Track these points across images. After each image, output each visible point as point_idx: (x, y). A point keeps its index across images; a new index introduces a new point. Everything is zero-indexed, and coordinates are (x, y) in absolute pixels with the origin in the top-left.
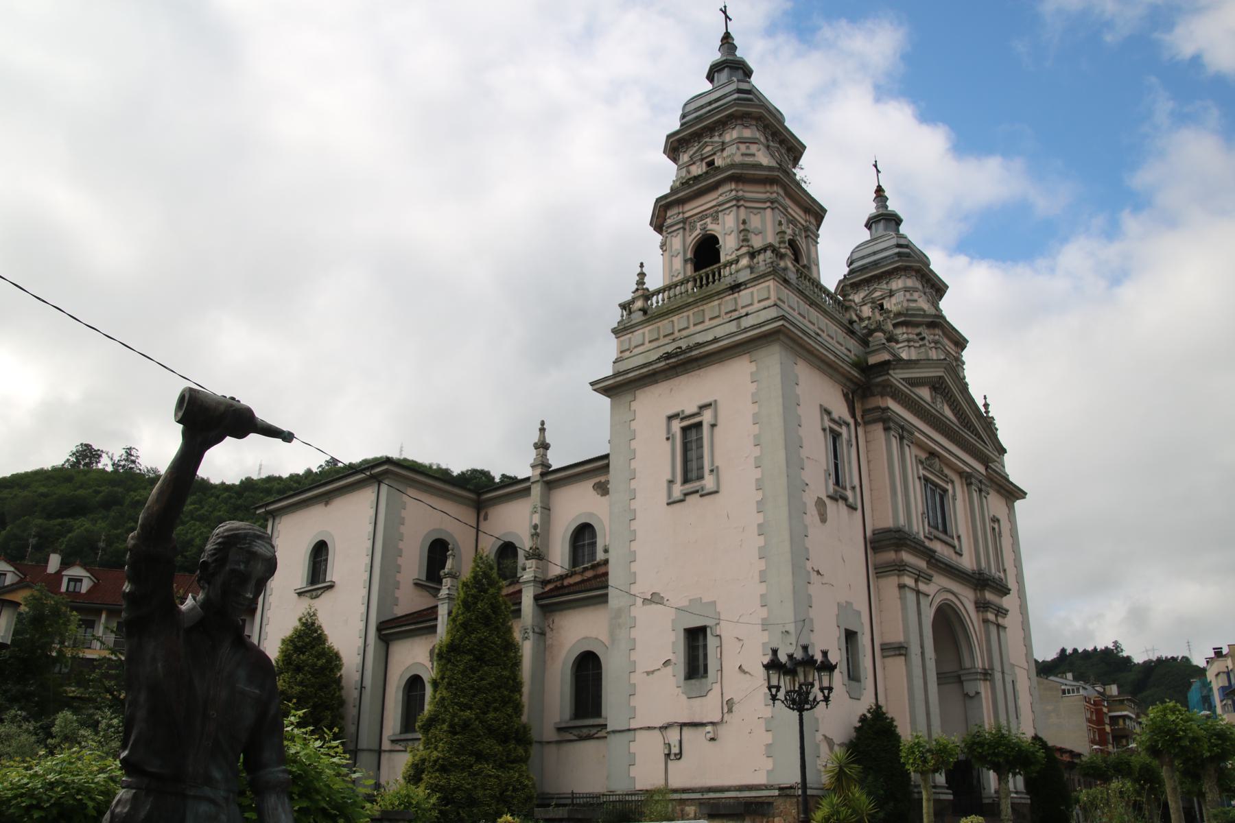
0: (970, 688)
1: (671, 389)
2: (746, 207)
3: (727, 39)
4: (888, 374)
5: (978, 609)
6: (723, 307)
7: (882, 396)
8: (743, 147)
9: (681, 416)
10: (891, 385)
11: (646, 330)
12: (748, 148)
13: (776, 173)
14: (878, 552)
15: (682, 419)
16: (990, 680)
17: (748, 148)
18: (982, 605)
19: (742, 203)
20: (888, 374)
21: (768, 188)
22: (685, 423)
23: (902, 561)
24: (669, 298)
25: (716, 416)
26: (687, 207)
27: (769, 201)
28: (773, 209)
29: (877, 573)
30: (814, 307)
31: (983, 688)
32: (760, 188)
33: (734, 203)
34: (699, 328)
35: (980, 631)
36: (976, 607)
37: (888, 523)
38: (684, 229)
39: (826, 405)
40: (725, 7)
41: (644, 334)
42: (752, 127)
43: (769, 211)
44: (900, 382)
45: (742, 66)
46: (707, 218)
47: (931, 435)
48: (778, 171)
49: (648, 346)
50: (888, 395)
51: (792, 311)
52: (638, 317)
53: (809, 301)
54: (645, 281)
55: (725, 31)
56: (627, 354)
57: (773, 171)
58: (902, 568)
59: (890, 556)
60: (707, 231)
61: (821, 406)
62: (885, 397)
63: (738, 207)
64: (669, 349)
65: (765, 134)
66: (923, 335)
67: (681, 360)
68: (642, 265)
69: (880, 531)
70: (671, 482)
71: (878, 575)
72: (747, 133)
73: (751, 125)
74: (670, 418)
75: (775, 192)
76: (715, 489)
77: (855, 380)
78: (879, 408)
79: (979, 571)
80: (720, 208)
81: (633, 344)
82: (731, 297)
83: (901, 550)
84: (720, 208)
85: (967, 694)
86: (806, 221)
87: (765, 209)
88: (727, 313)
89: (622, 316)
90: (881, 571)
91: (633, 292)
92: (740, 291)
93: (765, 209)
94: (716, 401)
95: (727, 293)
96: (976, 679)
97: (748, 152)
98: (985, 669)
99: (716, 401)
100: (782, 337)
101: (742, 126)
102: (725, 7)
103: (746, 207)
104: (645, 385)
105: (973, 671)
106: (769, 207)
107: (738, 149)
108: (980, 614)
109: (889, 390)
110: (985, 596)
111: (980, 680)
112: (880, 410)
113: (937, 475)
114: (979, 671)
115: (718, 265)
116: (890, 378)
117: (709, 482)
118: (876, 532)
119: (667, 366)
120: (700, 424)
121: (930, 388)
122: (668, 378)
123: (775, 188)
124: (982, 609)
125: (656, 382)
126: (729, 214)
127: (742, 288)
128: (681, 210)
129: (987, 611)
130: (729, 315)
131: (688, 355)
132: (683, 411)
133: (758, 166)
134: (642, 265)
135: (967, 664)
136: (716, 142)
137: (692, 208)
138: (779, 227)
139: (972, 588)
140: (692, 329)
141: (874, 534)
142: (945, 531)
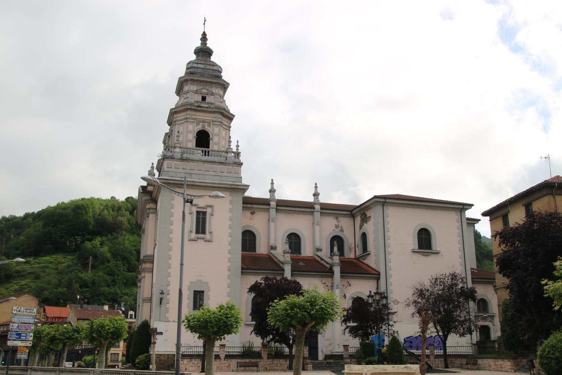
2: (178, 124)
19: (177, 123)
28: (186, 122)
43: (185, 123)
63: (175, 125)
87: (184, 122)
93: (184, 122)
103: (178, 124)
107: (183, 97)
123: (188, 112)
126: (181, 126)
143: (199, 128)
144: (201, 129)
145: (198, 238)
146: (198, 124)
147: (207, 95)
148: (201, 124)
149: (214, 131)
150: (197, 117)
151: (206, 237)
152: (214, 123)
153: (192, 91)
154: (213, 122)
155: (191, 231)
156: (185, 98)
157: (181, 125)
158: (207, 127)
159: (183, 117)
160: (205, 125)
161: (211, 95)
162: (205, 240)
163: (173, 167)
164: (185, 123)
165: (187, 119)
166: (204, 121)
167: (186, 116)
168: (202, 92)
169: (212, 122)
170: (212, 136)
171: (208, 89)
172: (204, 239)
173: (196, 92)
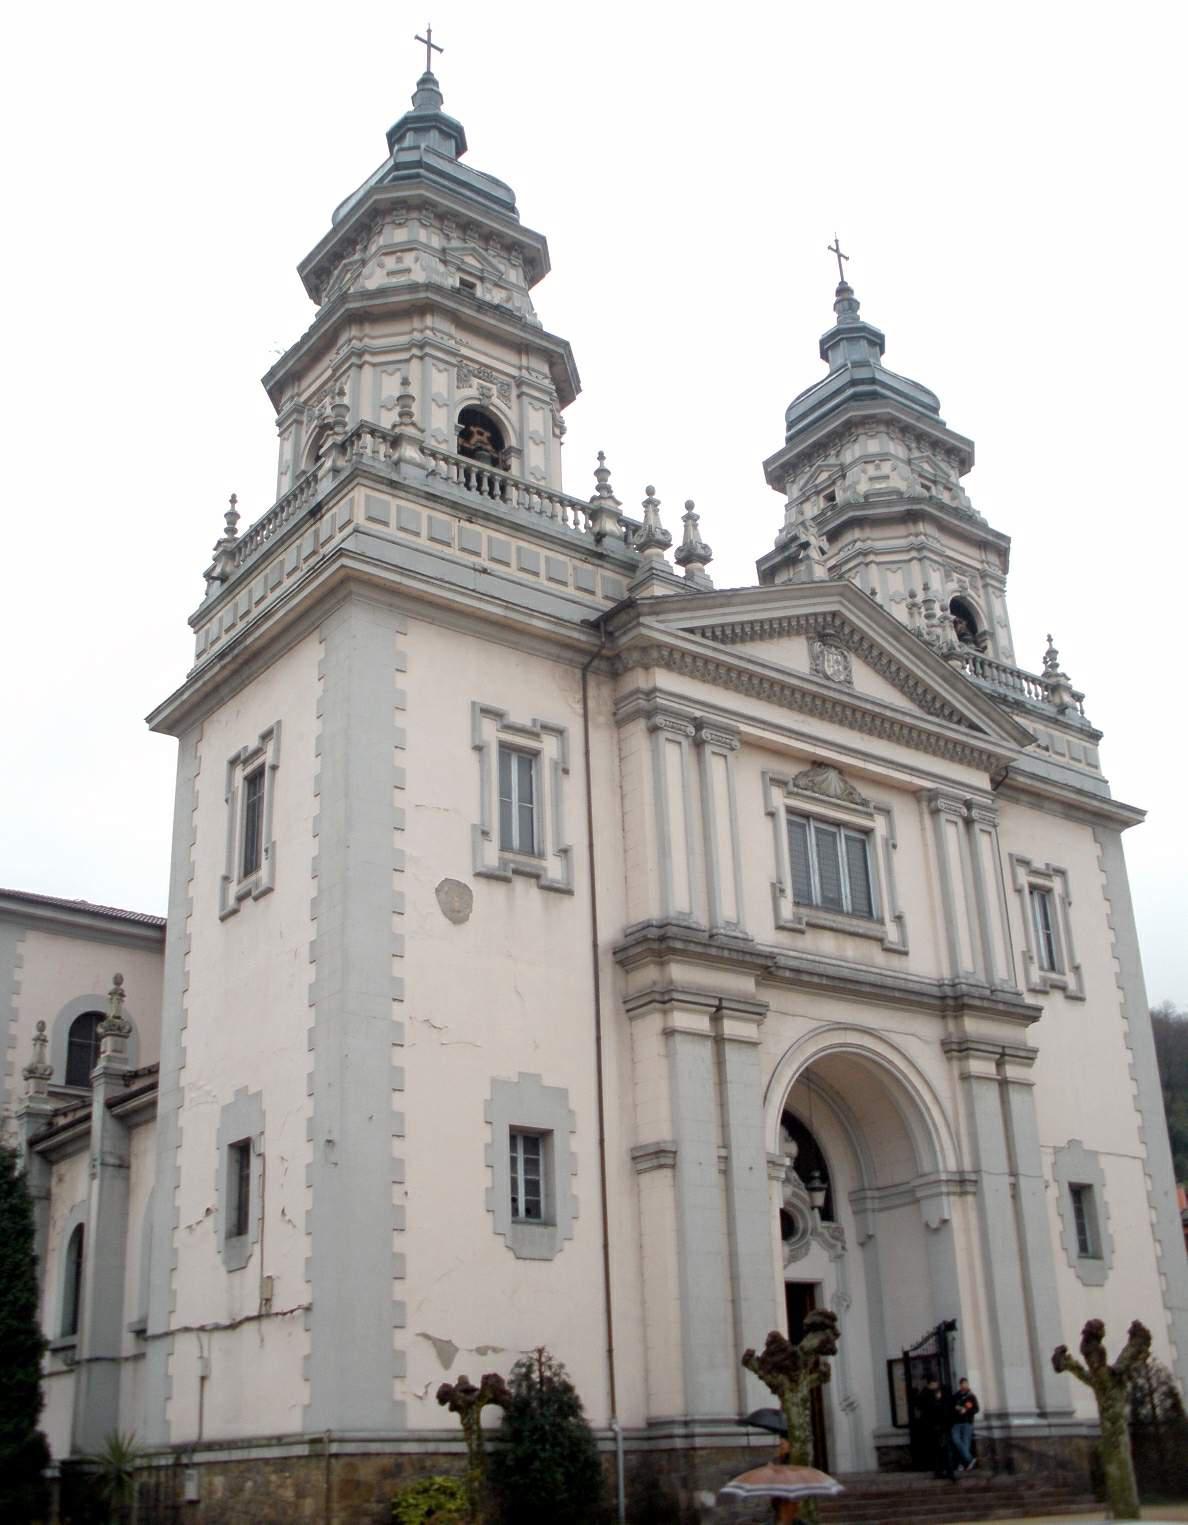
0: (931, 1213)
1: (238, 712)
2: (374, 365)
3: (427, 83)
4: (640, 624)
5: (949, 1055)
7: (646, 668)
8: (390, 263)
9: (242, 757)
10: (660, 646)
12: (399, 260)
13: (422, 295)
14: (632, 970)
15: (245, 762)
16: (974, 1194)
17: (399, 260)
18: (955, 1047)
19: (367, 357)
20: (640, 624)
21: (417, 323)
22: (250, 769)
23: (671, 982)
26: (305, 383)
27: (414, 345)
28: (421, 358)
29: (628, 1011)
30: (481, 521)
31: (956, 1211)
32: (404, 327)
33: (354, 360)
35: (954, 1098)
36: (946, 1052)
37: (652, 912)
38: (301, 423)
40: (429, 31)
42: (410, 223)
43: (415, 362)
44: (677, 637)
45: (434, 124)
46: (325, 397)
47: (805, 729)
48: (427, 290)
50: (659, 666)
51: (414, 538)
53: (464, 512)
54: (237, 526)
55: (425, 70)
57: (418, 292)
58: (666, 998)
59: (647, 975)
60: (324, 419)
61: (474, 704)
62: (651, 670)
63: (360, 367)
65: (441, 230)
66: (803, 539)
67: (237, 656)
68: (233, 500)
69: (635, 929)
70: (226, 879)
71: (631, 1013)
72: (400, 235)
73: (407, 220)
75: (427, 328)
77: (587, 647)
78: (638, 691)
79: (952, 980)
83: (667, 962)
85: (927, 1226)
86: (520, 368)
87: (408, 361)
90: (634, 1006)
91: (215, 549)
92: (322, 517)
93: (408, 361)
95: (307, 525)
96: (941, 1194)
97: (401, 266)
98: (961, 1172)
99: (279, 723)
100: (353, 587)
101: (394, 226)
102: (429, 31)
103: (374, 365)
104: (211, 711)
105: (933, 1178)
106: (413, 356)
107: (381, 265)
108: (955, 1064)
109: (655, 654)
110: (963, 1026)
111: (948, 1194)
112: (641, 696)
113: (838, 806)
114: (943, 1177)
116: (644, 631)
118: (629, 931)
119: (226, 672)
121: (808, 639)
122: (235, 692)
123: (429, 320)
124: (955, 1054)
125: (222, 703)
127: (323, 511)
128: (296, 390)
129: (967, 1057)
130: (308, 563)
132: (245, 748)
133: (414, 287)
134: (233, 500)
135: (927, 1167)
136: (356, 262)
138: (402, 387)
139: (937, 1016)
141: (626, 936)
142: (868, 914)
143: (469, 394)
144: (477, 402)
145: (516, 872)
146: (462, 380)
147: (482, 279)
148: (475, 381)
149: (521, 419)
150: (464, 351)
151: (545, 869)
152: (525, 389)
153: (427, 247)
154: (519, 386)
155: (486, 829)
156: (390, 274)
157: (391, 368)
158: (495, 400)
159: (404, 339)
160: (489, 389)
161: (496, 285)
162: (543, 882)
163: (393, 523)
164: (415, 362)
165: (421, 347)
166: (485, 372)
167: (417, 336)
168: (463, 262)
169: (513, 385)
170: (520, 437)
171: (485, 259)
172: (537, 877)
173: (444, 256)
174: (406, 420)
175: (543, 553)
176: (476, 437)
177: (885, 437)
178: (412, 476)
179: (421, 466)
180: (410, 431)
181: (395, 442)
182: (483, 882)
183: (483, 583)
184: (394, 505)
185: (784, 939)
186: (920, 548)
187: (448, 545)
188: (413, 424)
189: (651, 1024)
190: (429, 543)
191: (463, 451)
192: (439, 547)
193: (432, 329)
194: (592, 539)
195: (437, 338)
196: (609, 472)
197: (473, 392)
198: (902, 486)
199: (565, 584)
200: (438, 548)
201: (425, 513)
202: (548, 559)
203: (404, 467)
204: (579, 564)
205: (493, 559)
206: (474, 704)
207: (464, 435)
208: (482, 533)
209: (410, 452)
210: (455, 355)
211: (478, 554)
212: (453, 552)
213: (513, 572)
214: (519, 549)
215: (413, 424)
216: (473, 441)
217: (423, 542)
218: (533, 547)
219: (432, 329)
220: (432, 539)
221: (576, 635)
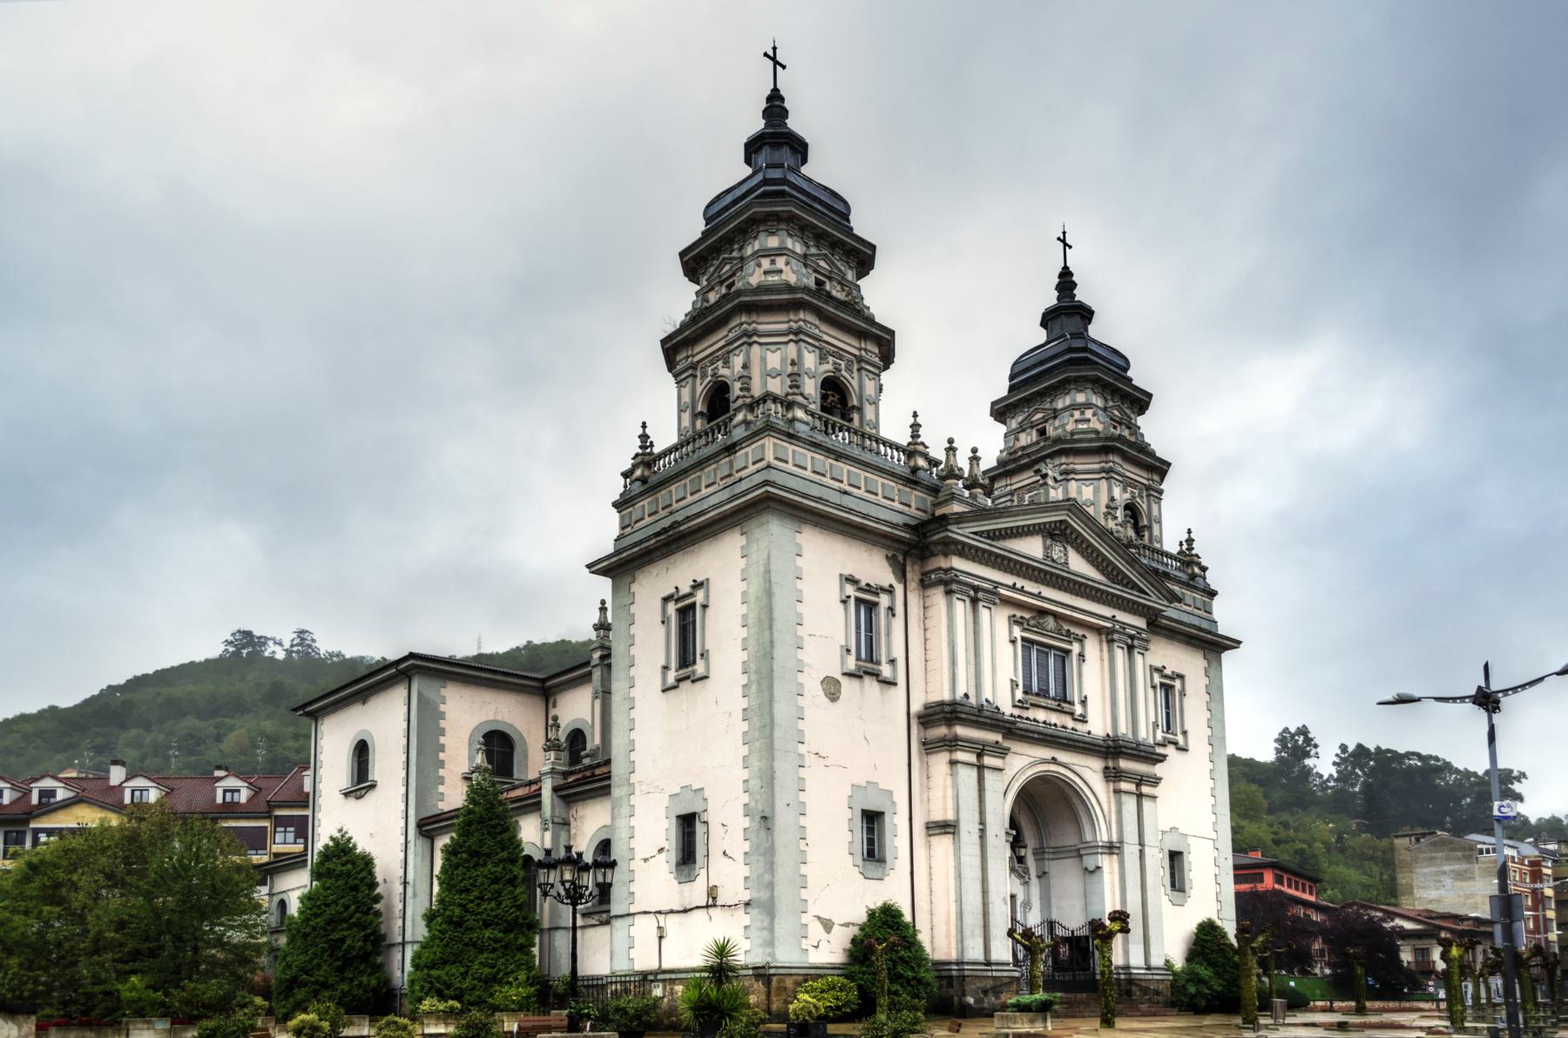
6: (718, 472)
11: (645, 502)
21: (792, 317)
24: (676, 461)
25: (707, 596)
34: (697, 497)
39: (846, 572)
41: (643, 506)
49: (648, 520)
52: (638, 487)
56: (628, 530)
61: (841, 575)
64: (666, 523)
74: (666, 600)
75: (800, 320)
76: (705, 674)
80: (731, 348)
81: (634, 519)
82: (727, 459)
84: (731, 348)
87: (787, 343)
88: (722, 479)
89: (625, 486)
93: (787, 343)
94: (708, 580)
106: (791, 340)
115: (728, 415)
117: (700, 668)
120: (693, 606)
131: (676, 530)
133: (788, 288)
137: (703, 350)
140: (690, 499)
159: (784, 326)
165: (796, 334)
174: (796, 390)
175: (879, 481)
176: (831, 398)
177: (1090, 391)
178: (802, 430)
179: (807, 424)
180: (800, 399)
181: (789, 406)
182: (846, 678)
183: (847, 501)
184: (790, 449)
185: (1016, 712)
186: (1111, 470)
187: (824, 475)
188: (802, 394)
189: (940, 761)
190: (812, 474)
191: (823, 409)
192: (819, 477)
193: (804, 321)
194: (908, 471)
195: (808, 328)
196: (920, 426)
197: (829, 367)
198: (1100, 427)
199: (893, 500)
200: (817, 478)
201: (809, 454)
202: (883, 484)
203: (798, 425)
204: (901, 487)
205: (851, 485)
206: (841, 575)
207: (824, 397)
208: (844, 468)
209: (800, 414)
210: (819, 340)
211: (841, 482)
212: (827, 481)
213: (861, 493)
214: (866, 478)
215: (802, 394)
216: (829, 401)
217: (808, 474)
218: (875, 477)
219: (804, 321)
220: (814, 472)
221: (903, 534)
